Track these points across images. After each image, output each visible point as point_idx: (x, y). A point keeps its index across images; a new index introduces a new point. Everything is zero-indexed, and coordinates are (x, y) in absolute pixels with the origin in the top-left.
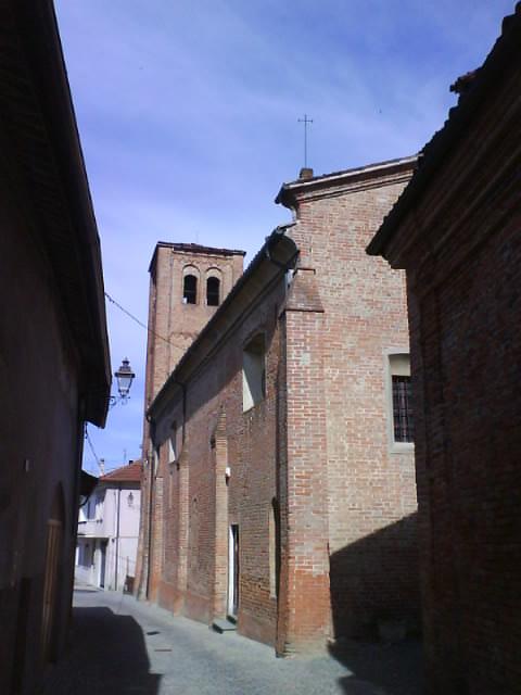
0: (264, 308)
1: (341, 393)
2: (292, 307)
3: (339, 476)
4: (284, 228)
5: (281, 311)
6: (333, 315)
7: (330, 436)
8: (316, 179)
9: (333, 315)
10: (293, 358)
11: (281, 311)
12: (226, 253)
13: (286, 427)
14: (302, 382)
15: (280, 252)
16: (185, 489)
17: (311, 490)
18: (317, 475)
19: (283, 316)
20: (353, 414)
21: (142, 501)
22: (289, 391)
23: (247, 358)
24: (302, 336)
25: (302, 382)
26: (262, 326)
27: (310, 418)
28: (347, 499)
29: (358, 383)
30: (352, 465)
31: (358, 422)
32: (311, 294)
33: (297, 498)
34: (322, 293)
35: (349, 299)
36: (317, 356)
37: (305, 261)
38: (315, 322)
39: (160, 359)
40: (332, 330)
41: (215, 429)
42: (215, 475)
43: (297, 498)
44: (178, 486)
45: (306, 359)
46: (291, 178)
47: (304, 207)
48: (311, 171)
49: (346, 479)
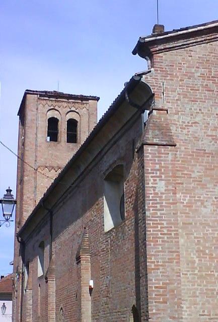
0: (122, 143)
1: (191, 214)
2: (149, 142)
3: (191, 287)
4: (140, 75)
5: (138, 145)
6: (183, 148)
7: (183, 253)
8: (167, 33)
9: (183, 148)
10: (150, 185)
11: (138, 145)
12: (83, 99)
13: (145, 245)
14: (158, 206)
15: (137, 95)
16: (53, 299)
17: (168, 299)
18: (172, 286)
19: (141, 150)
20: (202, 233)
21: (13, 310)
22: (147, 213)
23: (107, 186)
24: (157, 167)
25: (158, 206)
26: (121, 159)
27: (166, 237)
28: (198, 307)
29: (205, 207)
30: (201, 277)
31: (206, 241)
32: (165, 130)
33: (156, 306)
34: (173, 129)
35: (196, 135)
36: (171, 184)
37: (158, 103)
38: (169, 155)
39: (91, 127)
40: (182, 161)
41: (80, 248)
42: (80, 287)
43: (156, 306)
44: (46, 298)
45: (161, 186)
46: (146, 33)
47: (157, 58)
48: (163, 27)
49: (197, 289)
